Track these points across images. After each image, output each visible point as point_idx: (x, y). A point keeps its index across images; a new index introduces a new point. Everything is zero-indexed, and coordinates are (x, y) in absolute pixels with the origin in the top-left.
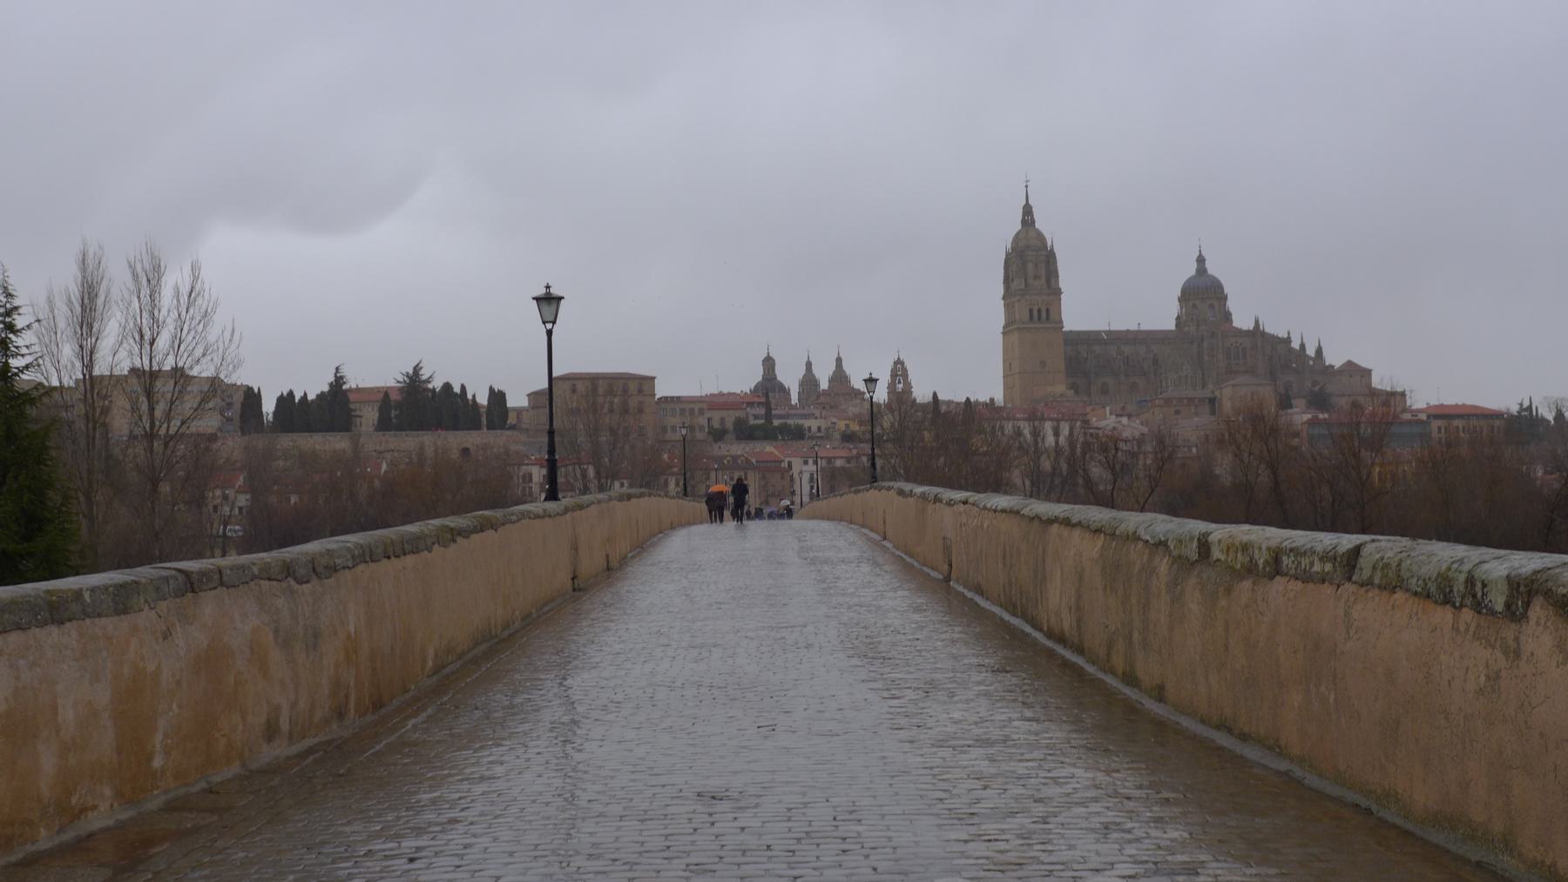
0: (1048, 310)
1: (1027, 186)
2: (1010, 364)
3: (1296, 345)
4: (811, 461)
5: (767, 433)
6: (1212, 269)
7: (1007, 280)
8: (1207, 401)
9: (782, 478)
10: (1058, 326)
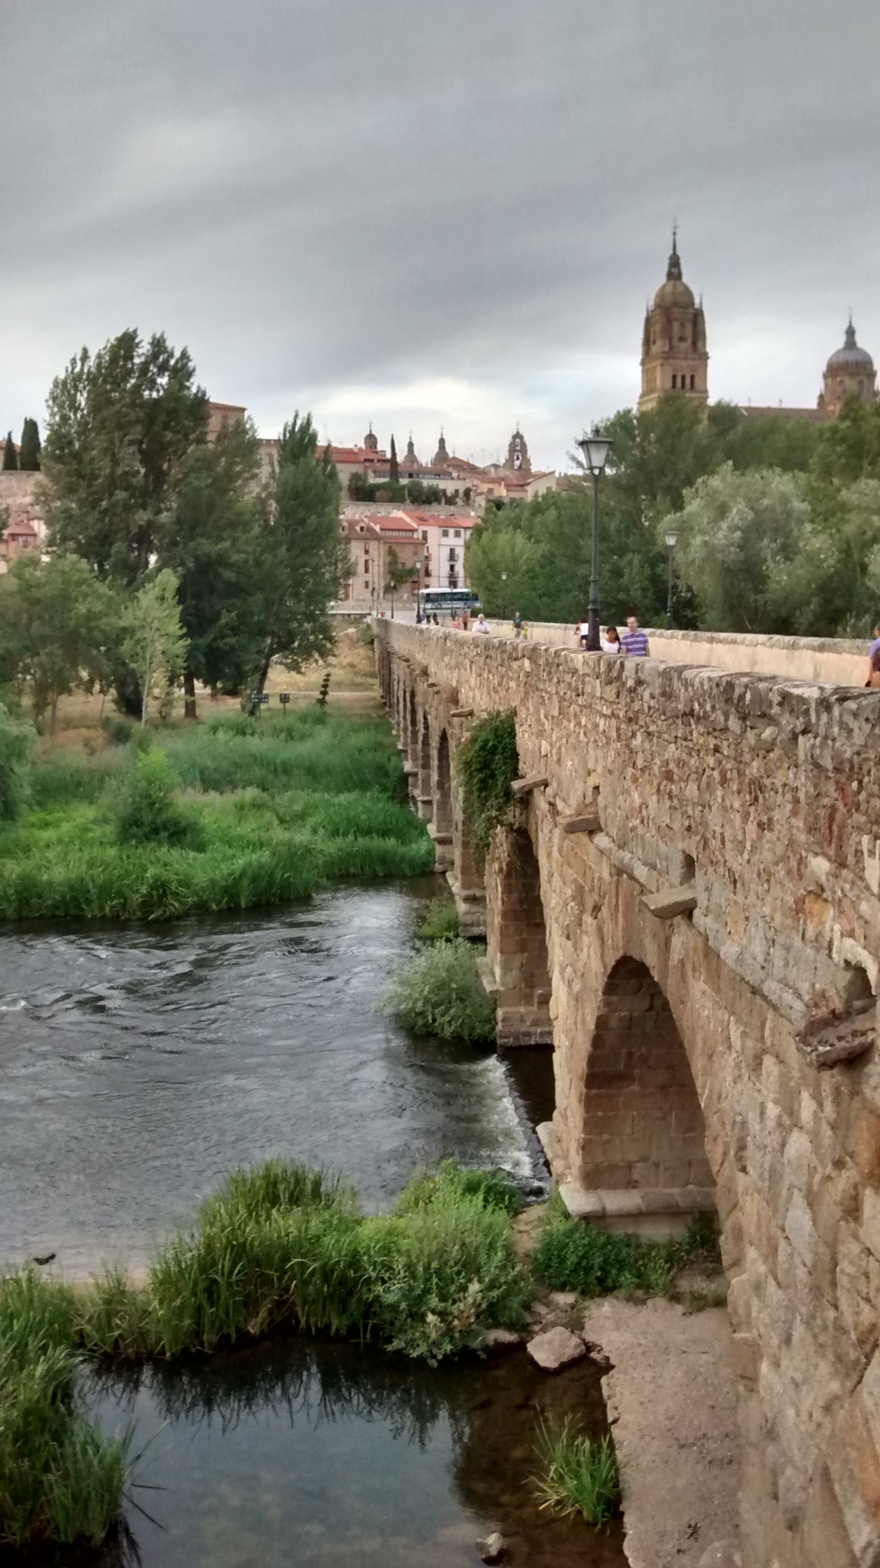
0: (692, 378)
1: (674, 234)
4: (451, 532)
5: (395, 496)
6: (861, 342)
7: (647, 342)
9: (415, 554)
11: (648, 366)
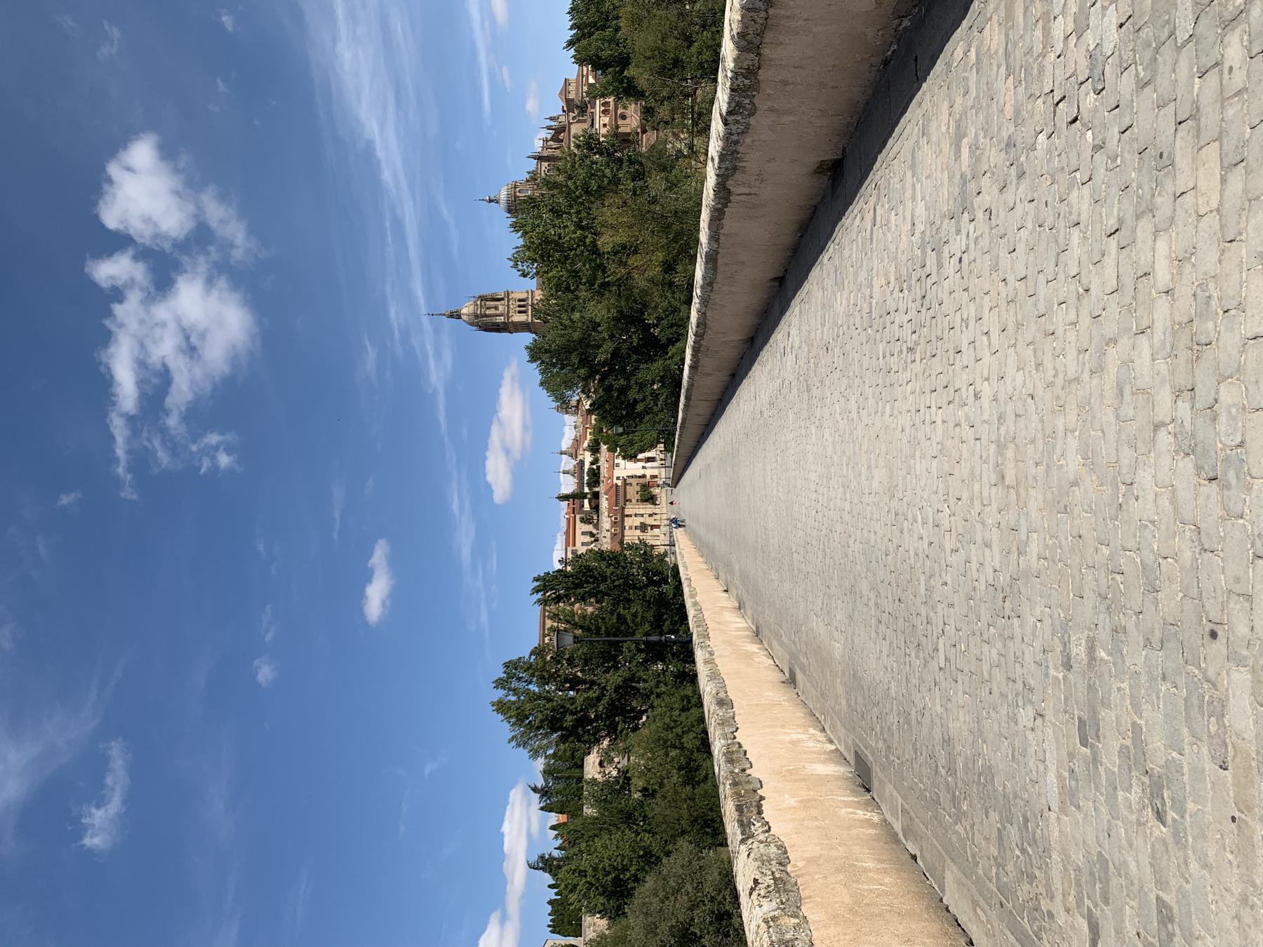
4: (616, 461)
9: (631, 484)
11: (512, 329)
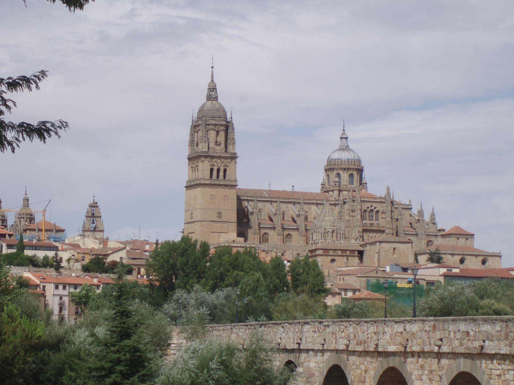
0: (225, 171)
2: (192, 213)
3: (415, 211)
8: (356, 253)
10: (234, 184)
